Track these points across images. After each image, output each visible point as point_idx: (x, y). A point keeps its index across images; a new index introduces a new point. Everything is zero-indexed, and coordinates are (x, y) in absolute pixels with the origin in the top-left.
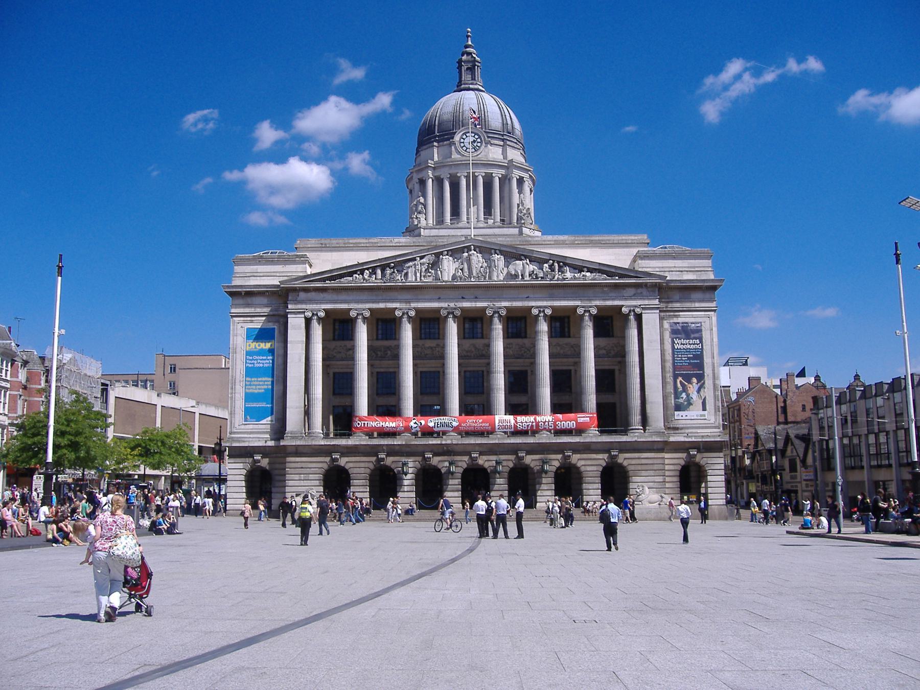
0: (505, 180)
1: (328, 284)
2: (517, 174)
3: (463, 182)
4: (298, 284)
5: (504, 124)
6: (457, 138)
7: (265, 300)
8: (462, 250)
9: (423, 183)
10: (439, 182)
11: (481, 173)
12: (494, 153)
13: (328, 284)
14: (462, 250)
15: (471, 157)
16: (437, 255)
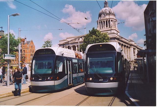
0: (109, 21)
1: (68, 43)
2: (111, 20)
3: (103, 22)
4: (65, 43)
5: (109, 12)
6: (102, 16)
7: (62, 46)
8: (82, 37)
9: (98, 23)
10: (100, 23)
11: (105, 21)
12: (107, 17)
13: (68, 43)
14: (82, 37)
15: (104, 18)
16: (79, 38)
